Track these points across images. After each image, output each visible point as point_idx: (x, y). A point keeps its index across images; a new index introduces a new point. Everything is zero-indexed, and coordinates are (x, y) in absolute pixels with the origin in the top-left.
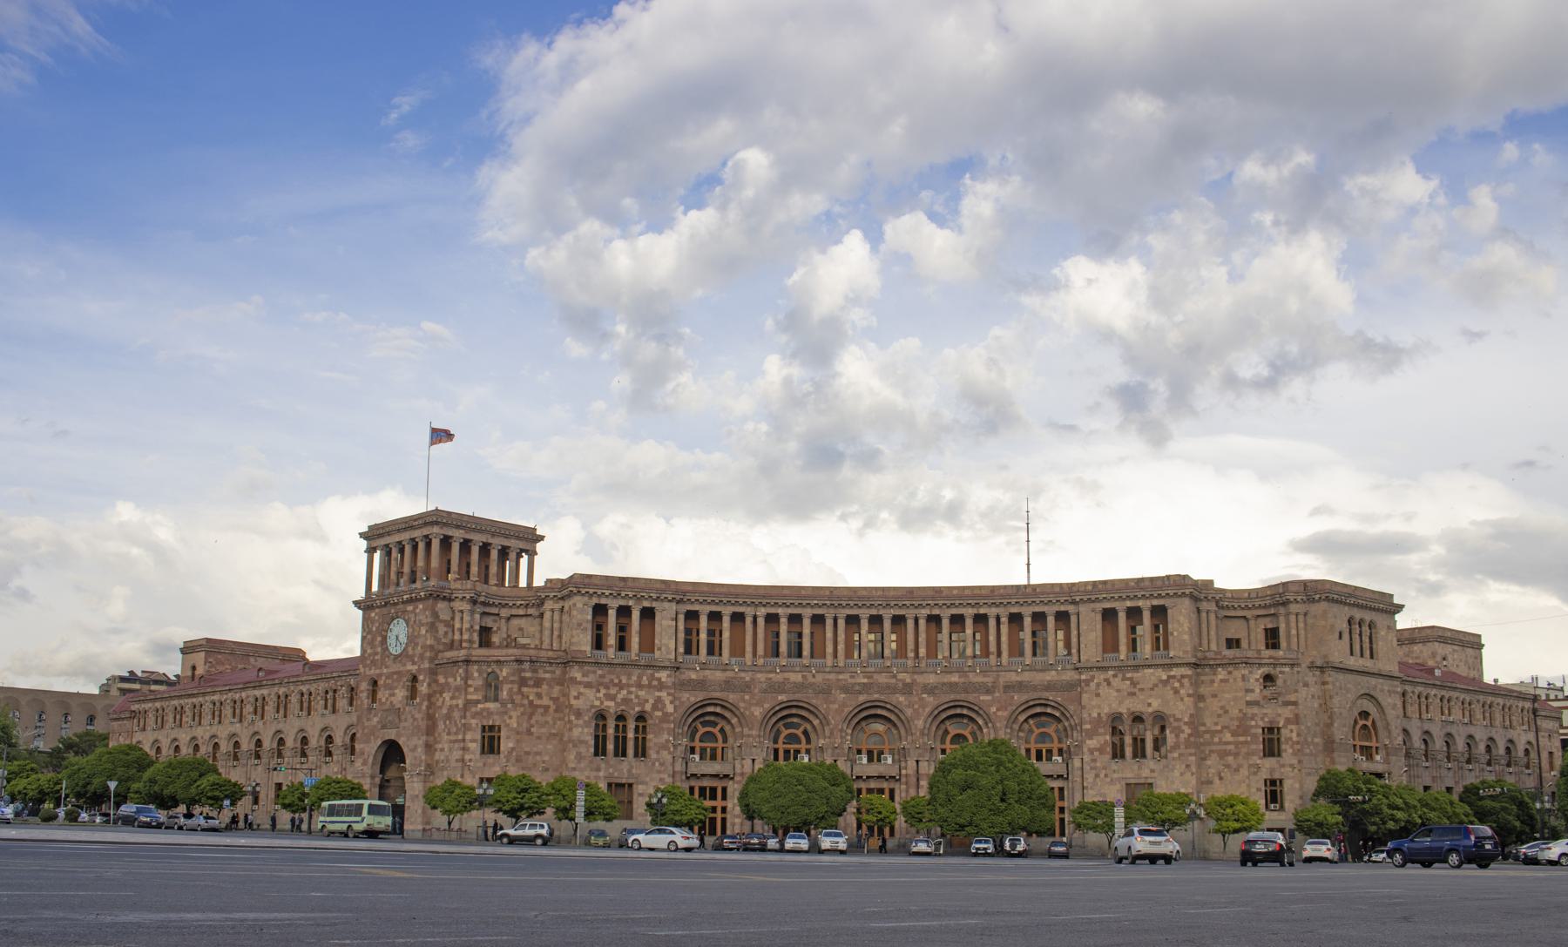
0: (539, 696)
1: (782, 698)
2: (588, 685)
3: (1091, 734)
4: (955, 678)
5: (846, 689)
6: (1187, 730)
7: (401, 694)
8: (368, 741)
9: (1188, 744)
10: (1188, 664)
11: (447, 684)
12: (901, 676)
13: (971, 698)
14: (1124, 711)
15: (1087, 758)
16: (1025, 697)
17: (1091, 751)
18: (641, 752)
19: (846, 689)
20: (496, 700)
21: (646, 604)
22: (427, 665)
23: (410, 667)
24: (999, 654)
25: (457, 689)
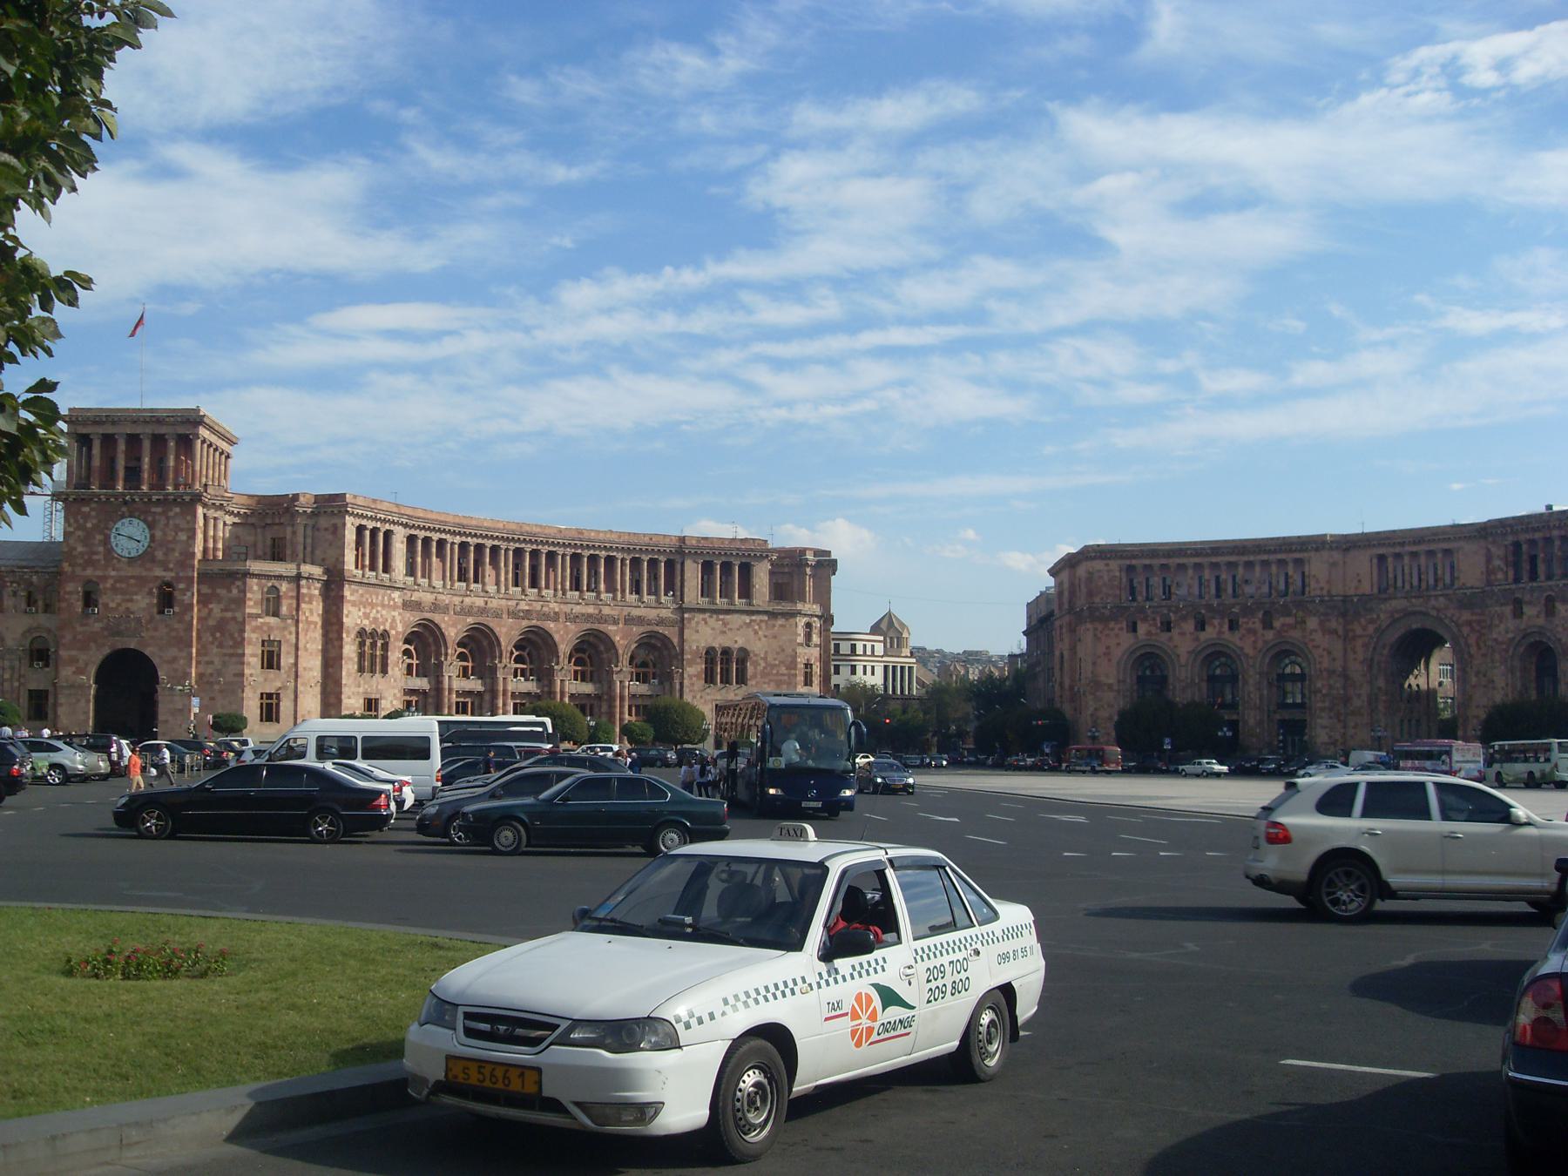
0: (311, 611)
1: (470, 620)
2: (354, 604)
4: (591, 610)
5: (513, 614)
7: (143, 603)
9: (764, 675)
10: (766, 612)
12: (552, 605)
13: (602, 627)
15: (686, 682)
16: (642, 629)
17: (690, 677)
18: (384, 671)
19: (513, 614)
20: (276, 614)
21: (387, 526)
23: (158, 572)
24: (623, 591)
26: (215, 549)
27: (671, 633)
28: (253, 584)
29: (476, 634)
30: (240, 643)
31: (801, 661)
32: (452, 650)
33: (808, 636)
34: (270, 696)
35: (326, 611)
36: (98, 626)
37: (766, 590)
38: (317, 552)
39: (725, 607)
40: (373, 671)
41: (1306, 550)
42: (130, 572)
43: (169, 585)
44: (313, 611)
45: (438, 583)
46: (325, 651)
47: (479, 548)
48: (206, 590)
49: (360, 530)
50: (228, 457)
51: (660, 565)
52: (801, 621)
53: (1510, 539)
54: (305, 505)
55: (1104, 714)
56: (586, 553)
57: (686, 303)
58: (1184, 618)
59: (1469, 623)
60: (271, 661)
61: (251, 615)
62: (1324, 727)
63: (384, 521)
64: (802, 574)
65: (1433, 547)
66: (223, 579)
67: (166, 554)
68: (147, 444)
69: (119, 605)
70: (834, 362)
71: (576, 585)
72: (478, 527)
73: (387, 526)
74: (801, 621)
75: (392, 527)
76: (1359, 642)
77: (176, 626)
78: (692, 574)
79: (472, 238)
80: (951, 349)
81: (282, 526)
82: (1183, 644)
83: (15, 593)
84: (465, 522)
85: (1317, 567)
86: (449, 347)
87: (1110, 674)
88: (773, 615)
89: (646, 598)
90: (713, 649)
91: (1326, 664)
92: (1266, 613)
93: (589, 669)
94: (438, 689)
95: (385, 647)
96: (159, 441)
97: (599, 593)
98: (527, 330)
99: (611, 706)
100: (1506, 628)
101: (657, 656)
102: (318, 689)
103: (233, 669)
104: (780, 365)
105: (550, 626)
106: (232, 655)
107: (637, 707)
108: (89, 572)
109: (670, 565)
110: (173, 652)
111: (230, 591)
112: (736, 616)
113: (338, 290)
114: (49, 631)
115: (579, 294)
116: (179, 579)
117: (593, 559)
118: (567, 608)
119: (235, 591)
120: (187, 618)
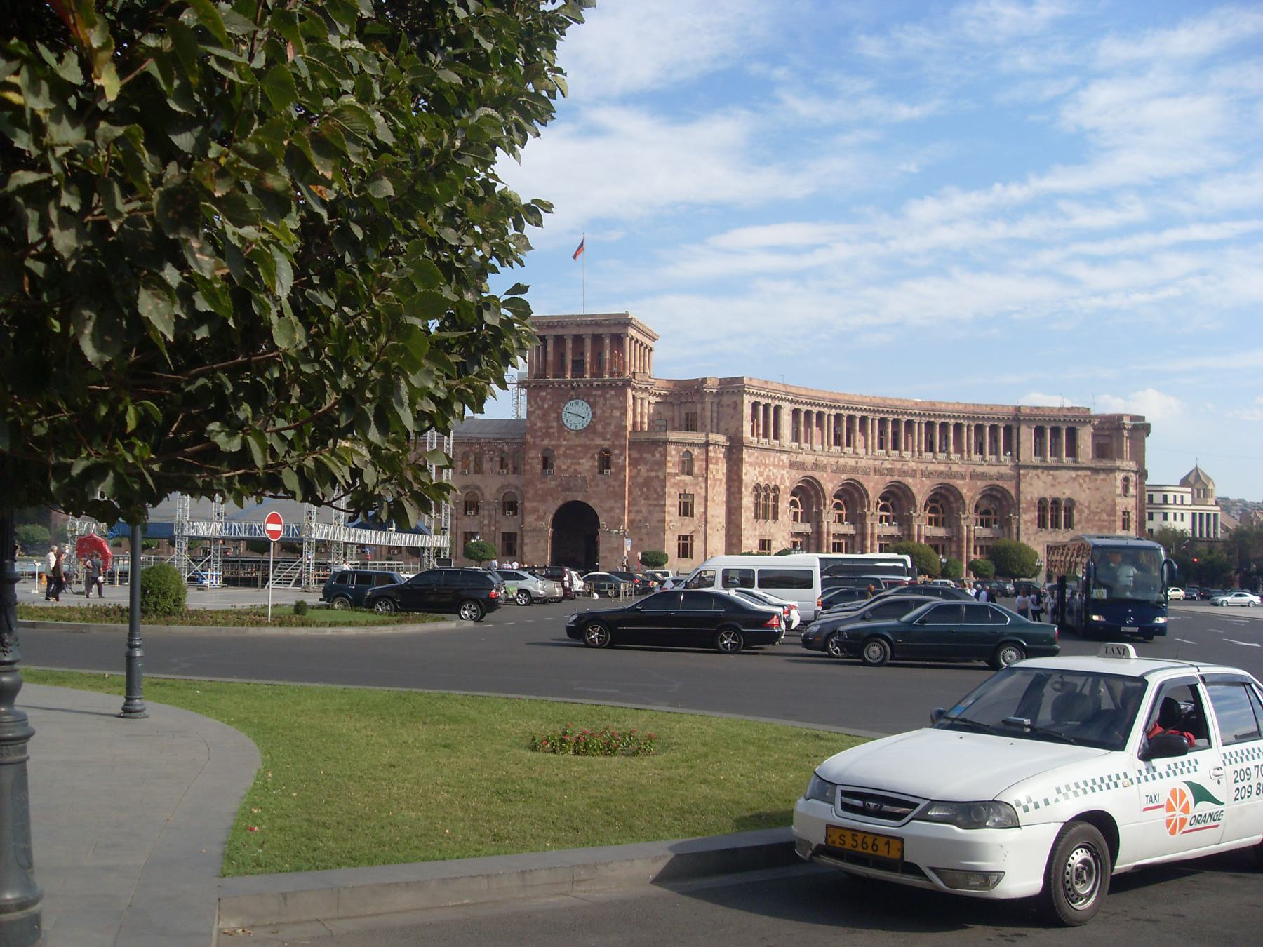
0: (717, 471)
1: (844, 476)
2: (751, 465)
3: (1027, 511)
4: (942, 468)
5: (878, 471)
6: (1087, 511)
7: (587, 465)
8: (543, 499)
9: (1088, 520)
11: (642, 458)
13: (951, 482)
14: (1047, 496)
15: (1022, 527)
16: (985, 483)
17: (1026, 522)
18: (775, 518)
19: (878, 471)
20: (690, 473)
21: (777, 402)
23: (599, 441)
24: (969, 452)
26: (642, 423)
27: (1009, 486)
28: (672, 450)
29: (850, 488)
30: (662, 496)
31: (1119, 509)
32: (830, 501)
33: (1126, 489)
34: (685, 538)
35: (729, 470)
36: (553, 483)
37: (1089, 450)
38: (722, 424)
39: (1055, 464)
40: (766, 518)
42: (577, 441)
43: (607, 451)
44: (719, 470)
45: (817, 447)
46: (728, 502)
47: (851, 419)
48: (635, 455)
49: (755, 405)
50: (651, 350)
51: (999, 430)
52: (1120, 476)
54: (711, 387)
56: (938, 421)
57: (1012, 214)
60: (686, 510)
61: (670, 474)
63: (774, 398)
64: (1118, 437)
66: (649, 446)
67: (604, 427)
68: (588, 343)
70: (1141, 257)
71: (930, 447)
72: (849, 402)
73: (777, 402)
74: (1120, 476)
75: (780, 403)
78: (1027, 437)
79: (835, 169)
80: (1245, 241)
81: (692, 403)
83: (491, 459)
84: (839, 398)
86: (821, 257)
88: (1095, 471)
89: (988, 457)
90: (1045, 499)
93: (941, 516)
94: (818, 532)
95: (776, 499)
96: (597, 339)
97: (949, 454)
98: (883, 241)
99: (960, 547)
101: (997, 505)
102: (723, 532)
103: (656, 516)
104: (1094, 261)
105: (909, 481)
106: (655, 506)
107: (981, 547)
108: (546, 442)
109: (1008, 430)
110: (610, 503)
112: (1064, 472)
113: (730, 215)
114: (517, 488)
115: (924, 210)
116: (614, 446)
117: (944, 426)
118: (922, 467)
119: (658, 455)
120: (621, 477)
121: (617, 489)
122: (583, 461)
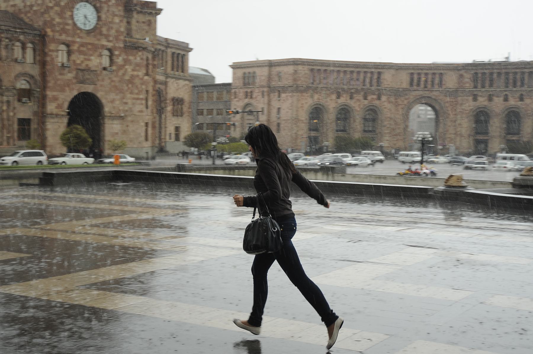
8: (63, 90)
20: (147, 74)
22: (122, 45)
23: (104, 42)
25: (138, 65)
41: (384, 69)
48: (124, 56)
53: (473, 72)
55: (300, 133)
58: (332, 93)
59: (447, 102)
62: (387, 140)
65: (435, 71)
67: (108, 30)
69: (82, 62)
76: (401, 106)
77: (115, 79)
82: (332, 104)
85: (387, 77)
87: (304, 116)
91: (389, 116)
92: (365, 93)
100: (469, 105)
106: (138, 99)
110: (112, 96)
111: (136, 59)
120: (121, 73)
121: (117, 84)
122: (92, 58)
